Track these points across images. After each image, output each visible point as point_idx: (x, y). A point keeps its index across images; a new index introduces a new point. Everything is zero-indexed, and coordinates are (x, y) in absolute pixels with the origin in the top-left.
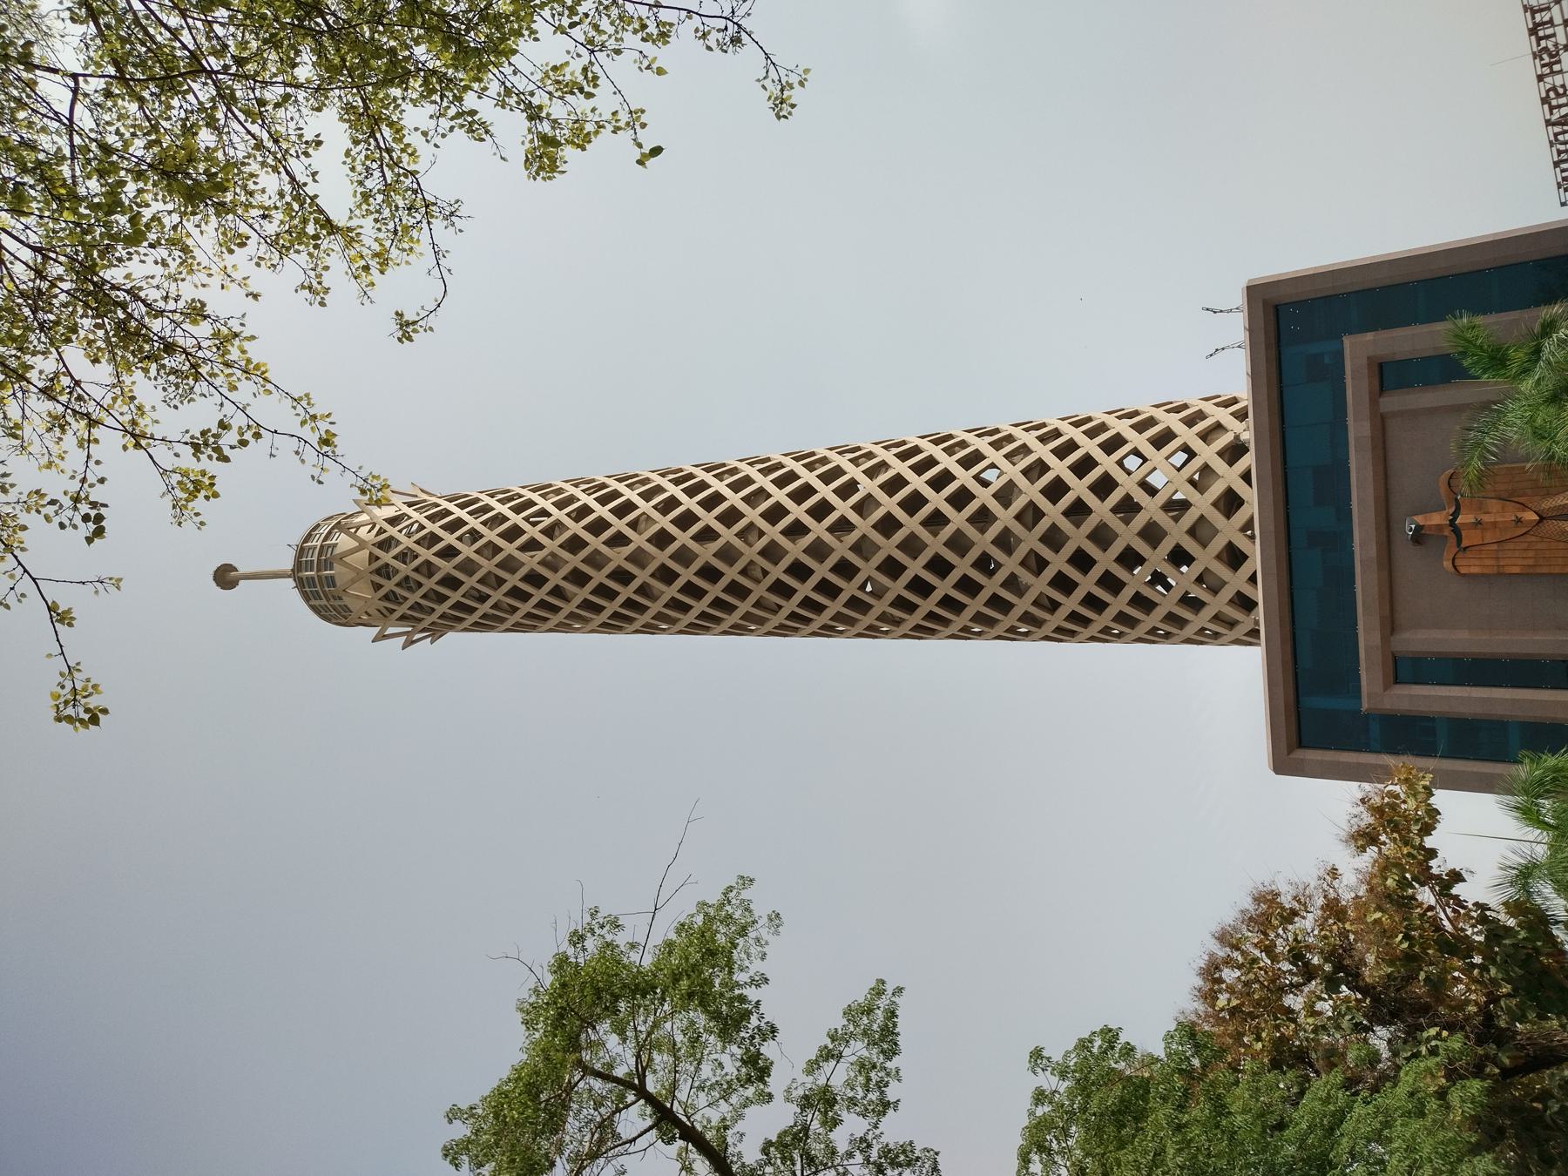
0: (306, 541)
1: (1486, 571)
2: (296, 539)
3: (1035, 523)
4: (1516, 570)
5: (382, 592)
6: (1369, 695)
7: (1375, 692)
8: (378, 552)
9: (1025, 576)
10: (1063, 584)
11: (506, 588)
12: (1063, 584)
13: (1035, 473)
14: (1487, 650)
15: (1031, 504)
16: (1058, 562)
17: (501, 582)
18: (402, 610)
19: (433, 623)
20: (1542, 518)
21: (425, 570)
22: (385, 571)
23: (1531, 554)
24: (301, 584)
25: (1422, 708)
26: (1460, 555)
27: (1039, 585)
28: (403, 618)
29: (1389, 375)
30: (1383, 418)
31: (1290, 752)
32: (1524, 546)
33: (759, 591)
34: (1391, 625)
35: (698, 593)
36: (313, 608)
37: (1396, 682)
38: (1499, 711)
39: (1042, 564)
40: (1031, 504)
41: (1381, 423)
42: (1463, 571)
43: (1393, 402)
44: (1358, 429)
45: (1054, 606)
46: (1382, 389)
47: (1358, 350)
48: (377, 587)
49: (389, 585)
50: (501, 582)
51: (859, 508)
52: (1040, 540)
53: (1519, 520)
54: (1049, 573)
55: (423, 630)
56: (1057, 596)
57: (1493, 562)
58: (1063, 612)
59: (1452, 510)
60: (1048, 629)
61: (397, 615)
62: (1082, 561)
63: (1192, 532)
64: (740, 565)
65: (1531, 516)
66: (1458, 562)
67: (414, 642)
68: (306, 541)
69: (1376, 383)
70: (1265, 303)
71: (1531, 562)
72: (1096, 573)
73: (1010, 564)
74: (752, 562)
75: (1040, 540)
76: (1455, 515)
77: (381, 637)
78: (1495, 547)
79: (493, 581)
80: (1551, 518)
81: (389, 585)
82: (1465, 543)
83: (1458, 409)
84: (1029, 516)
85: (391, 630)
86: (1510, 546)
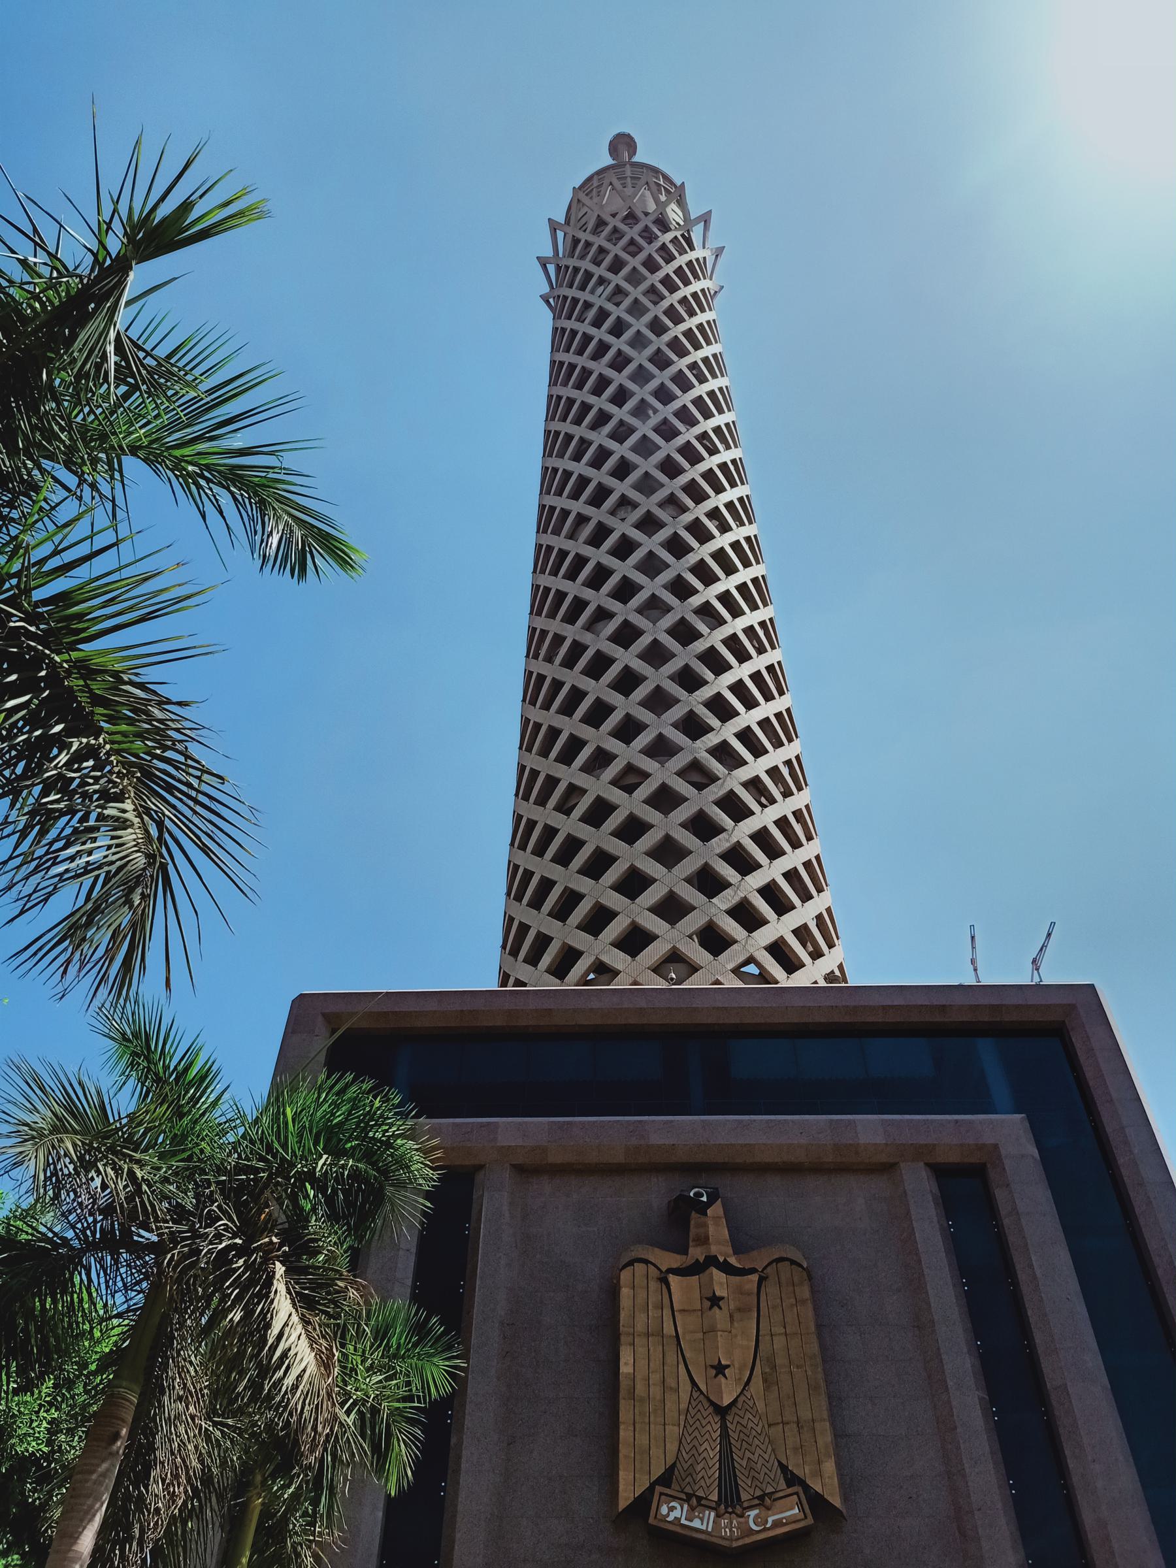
1: (623, 1315)
4: (625, 1369)
8: (652, 218)
20: (722, 1412)
23: (656, 1391)
30: (886, 1168)
32: (671, 1382)
42: (625, 1276)
43: (918, 1183)
44: (869, 1129)
46: (941, 1172)
47: (1007, 1133)
48: (614, 216)
49: (613, 222)
53: (720, 1369)
57: (640, 1327)
59: (733, 1260)
66: (640, 1268)
69: (953, 1158)
70: (1072, 1008)
71: (640, 1389)
76: (727, 1268)
77: (554, 226)
78: (669, 1329)
80: (724, 1428)
82: (672, 1279)
83: (915, 1284)
84: (697, 778)
86: (671, 1357)
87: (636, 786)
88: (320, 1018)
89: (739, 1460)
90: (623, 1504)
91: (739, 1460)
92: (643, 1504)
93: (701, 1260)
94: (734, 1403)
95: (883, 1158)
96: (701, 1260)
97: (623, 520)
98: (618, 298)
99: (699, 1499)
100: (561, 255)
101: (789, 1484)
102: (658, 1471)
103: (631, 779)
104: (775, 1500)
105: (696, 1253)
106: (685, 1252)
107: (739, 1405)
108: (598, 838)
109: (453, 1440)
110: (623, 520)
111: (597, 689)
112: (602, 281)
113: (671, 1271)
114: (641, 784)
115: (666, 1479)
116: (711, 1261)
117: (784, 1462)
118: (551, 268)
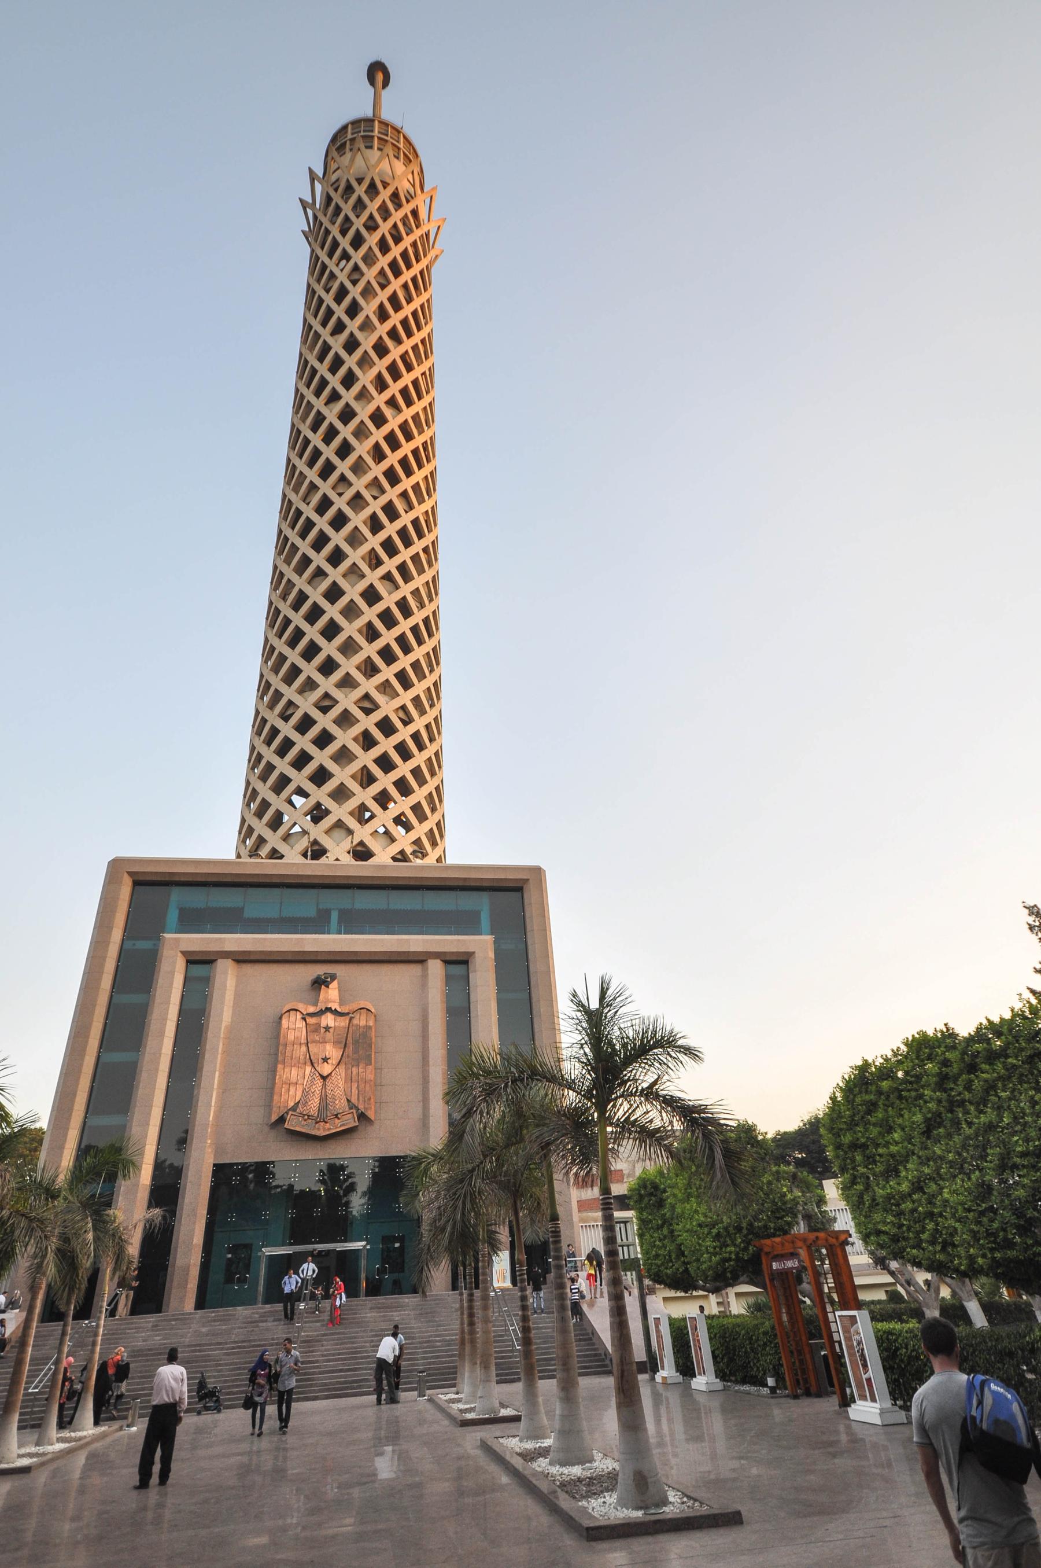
0: (405, 137)
2: (407, 130)
3: (361, 708)
5: (354, 184)
6: (177, 940)
7: (177, 945)
8: (390, 191)
9: (316, 695)
10: (305, 724)
11: (348, 285)
12: (305, 724)
13: (401, 714)
14: (210, 1035)
15: (377, 707)
16: (325, 722)
17: (354, 283)
18: (337, 198)
19: (321, 224)
20: (324, 1078)
21: (370, 223)
22: (372, 190)
24: (369, 121)
25: (161, 981)
27: (306, 704)
28: (329, 199)
29: (459, 963)
31: (131, 874)
33: (325, 487)
34: (242, 959)
35: (339, 298)
36: (345, 128)
37: (188, 961)
38: (150, 1044)
39: (325, 710)
40: (377, 707)
41: (418, 959)
45: (292, 643)
47: (481, 945)
49: (360, 190)
50: (354, 283)
51: (388, 577)
52: (346, 710)
53: (325, 1060)
54: (315, 714)
55: (315, 217)
56: (294, 720)
58: (280, 724)
59: (339, 1009)
60: (266, 713)
61: (332, 194)
62: (324, 740)
63: (339, 824)
64: (350, 475)
65: (326, 1069)
67: (305, 209)
68: (405, 137)
72: (312, 750)
73: (327, 684)
74: (350, 484)
75: (346, 710)
76: (336, 1013)
79: (355, 276)
80: (324, 1086)
81: (360, 190)
85: (318, 187)
87: (331, 707)
88: (126, 875)
92: (282, 1120)
94: (330, 1074)
97: (340, 495)
98: (355, 276)
100: (318, 206)
101: (351, 1108)
102: (291, 1104)
103: (326, 703)
105: (321, 1006)
106: (316, 1004)
108: (303, 742)
110: (340, 495)
111: (312, 633)
112: (346, 256)
113: (308, 1014)
114: (332, 706)
115: (294, 1108)
116: (329, 1010)
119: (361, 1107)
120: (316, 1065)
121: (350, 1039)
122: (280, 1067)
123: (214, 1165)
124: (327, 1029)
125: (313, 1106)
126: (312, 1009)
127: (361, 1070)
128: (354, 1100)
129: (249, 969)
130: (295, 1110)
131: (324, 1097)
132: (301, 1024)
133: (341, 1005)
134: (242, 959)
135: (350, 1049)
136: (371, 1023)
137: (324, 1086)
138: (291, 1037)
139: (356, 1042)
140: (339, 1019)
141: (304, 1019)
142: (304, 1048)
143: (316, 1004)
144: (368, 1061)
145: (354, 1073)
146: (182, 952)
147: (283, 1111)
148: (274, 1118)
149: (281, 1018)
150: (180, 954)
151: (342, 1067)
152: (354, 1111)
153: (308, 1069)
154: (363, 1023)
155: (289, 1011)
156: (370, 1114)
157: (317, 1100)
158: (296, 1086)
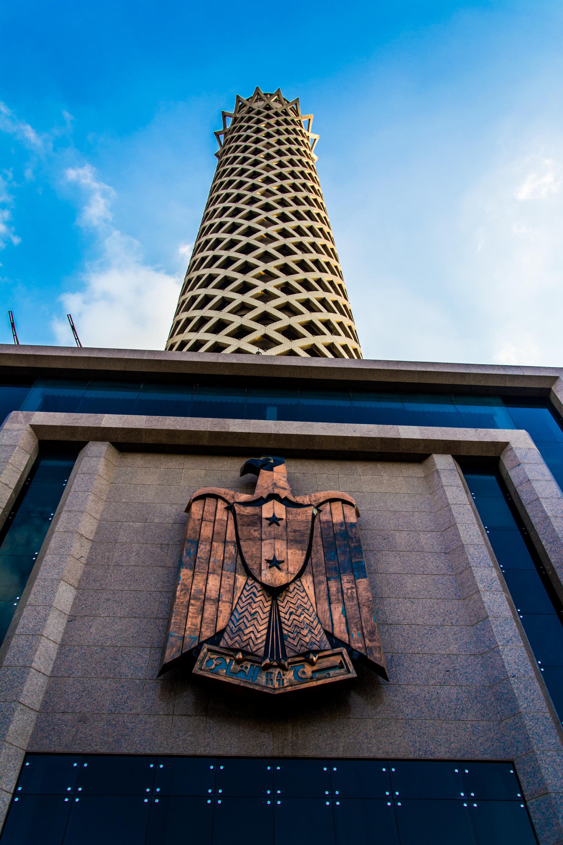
20: (275, 593)
26: (221, 505)
53: (274, 563)
59: (292, 498)
65: (277, 577)
66: (209, 501)
76: (286, 502)
80: (275, 610)
89: (287, 628)
90: (168, 658)
91: (287, 628)
92: (189, 657)
93: (265, 496)
94: (285, 588)
95: (420, 450)
96: (265, 496)
99: (245, 653)
102: (207, 633)
104: (319, 658)
105: (262, 490)
107: (291, 588)
109: (16, 615)
117: (330, 630)
118: (222, 137)
119: (357, 645)
120: (255, 573)
121: (317, 540)
122: (185, 573)
123: (29, 755)
124: (274, 520)
125: (257, 633)
126: (244, 497)
127: (346, 586)
128: (340, 631)
129: (138, 461)
130: (217, 644)
131: (275, 624)
132: (222, 515)
133: (292, 492)
134: (127, 444)
135: (319, 554)
136: (352, 519)
137: (275, 610)
138: (206, 531)
139: (330, 547)
140: (294, 510)
141: (230, 508)
142: (232, 549)
143: (252, 493)
144: (359, 570)
145: (333, 589)
146: (32, 426)
147: (191, 644)
148: (171, 654)
149: (188, 509)
150: (30, 429)
151: (307, 582)
152: (344, 651)
153: (241, 580)
154: (338, 518)
155: (202, 497)
156: (377, 657)
157: (263, 628)
158: (215, 599)
